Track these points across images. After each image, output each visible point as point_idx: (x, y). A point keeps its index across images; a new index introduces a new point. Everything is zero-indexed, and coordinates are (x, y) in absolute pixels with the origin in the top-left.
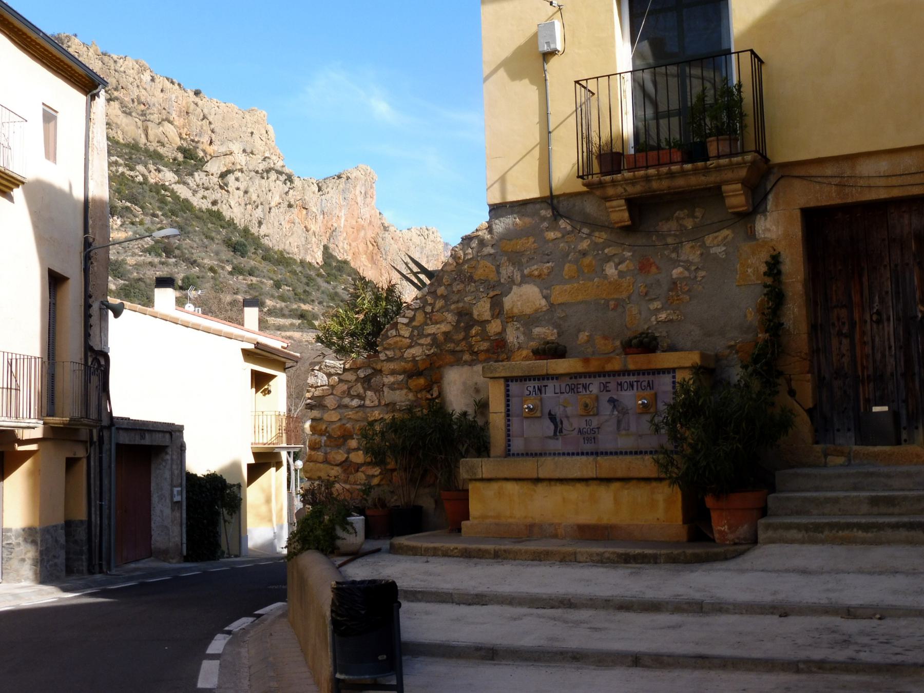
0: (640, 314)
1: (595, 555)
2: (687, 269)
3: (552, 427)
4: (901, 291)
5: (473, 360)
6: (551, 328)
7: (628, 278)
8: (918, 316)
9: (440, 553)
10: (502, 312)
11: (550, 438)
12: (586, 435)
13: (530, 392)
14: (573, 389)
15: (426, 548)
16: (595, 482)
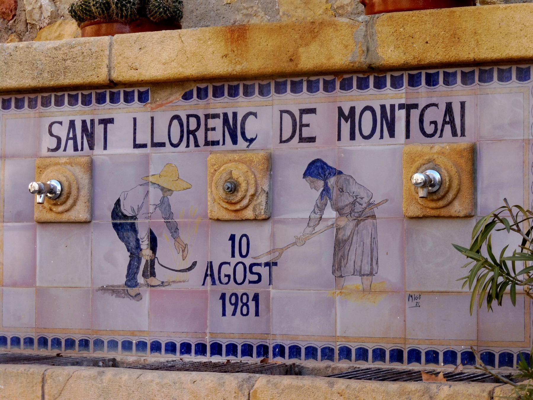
11: (113, 290)
12: (231, 288)
13: (59, 140)
14: (193, 133)
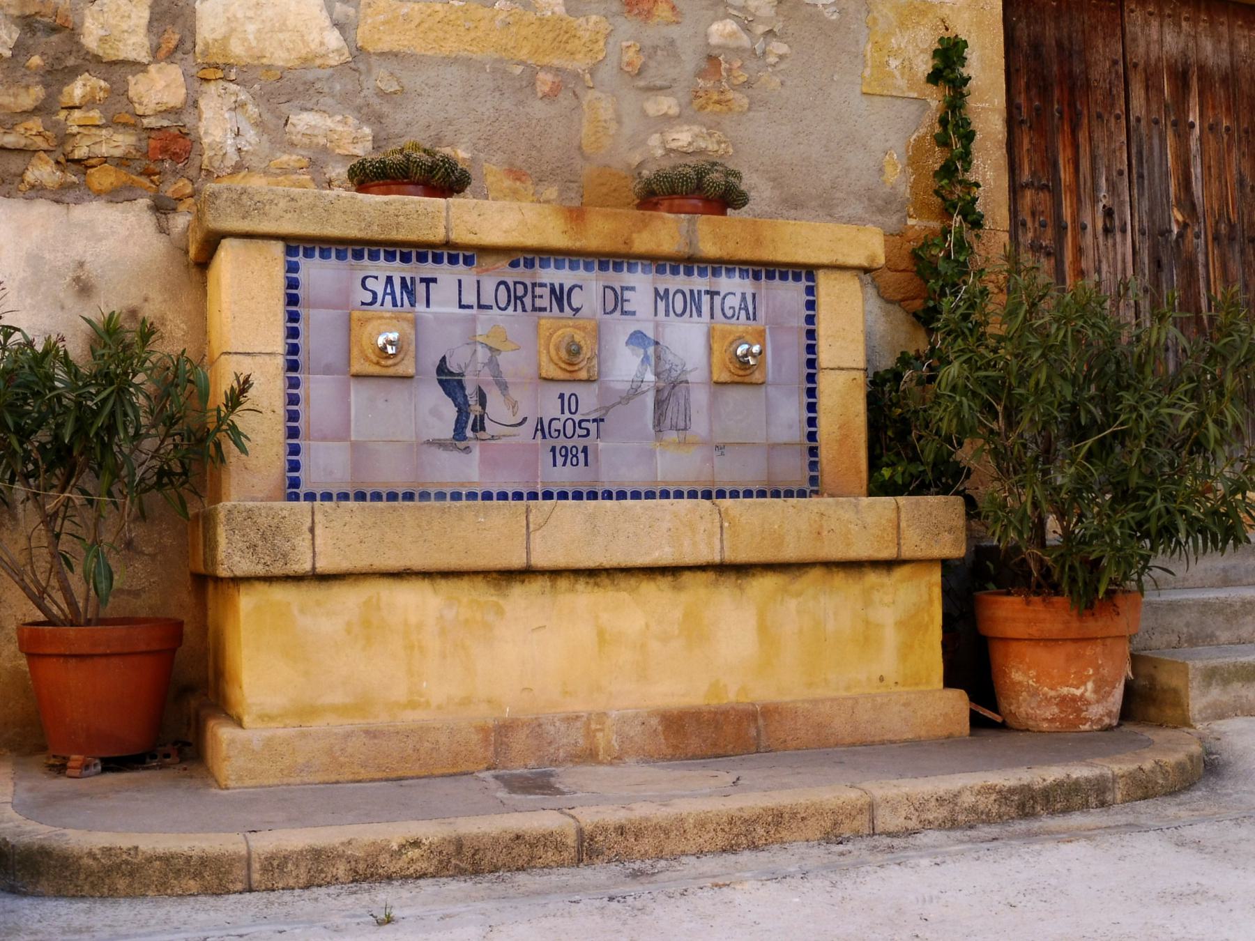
0: (619, 122)
1: (933, 803)
2: (747, 29)
3: (450, 411)
4: (1146, 174)
5: (65, 187)
6: (352, 120)
7: (594, 18)
8: (1170, 231)
9: (341, 869)
10: (188, 45)
11: (440, 444)
12: (561, 442)
13: (375, 294)
14: (521, 298)
15: (271, 858)
16: (702, 577)
